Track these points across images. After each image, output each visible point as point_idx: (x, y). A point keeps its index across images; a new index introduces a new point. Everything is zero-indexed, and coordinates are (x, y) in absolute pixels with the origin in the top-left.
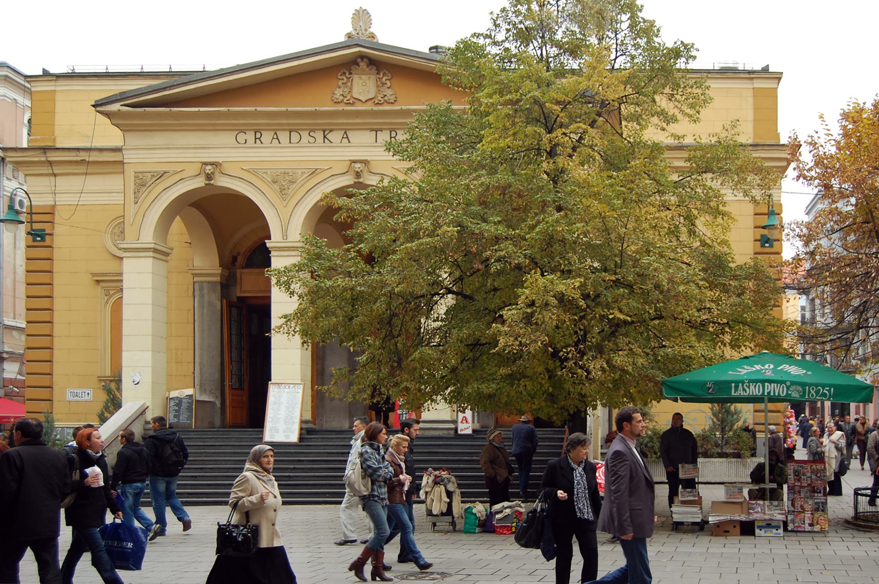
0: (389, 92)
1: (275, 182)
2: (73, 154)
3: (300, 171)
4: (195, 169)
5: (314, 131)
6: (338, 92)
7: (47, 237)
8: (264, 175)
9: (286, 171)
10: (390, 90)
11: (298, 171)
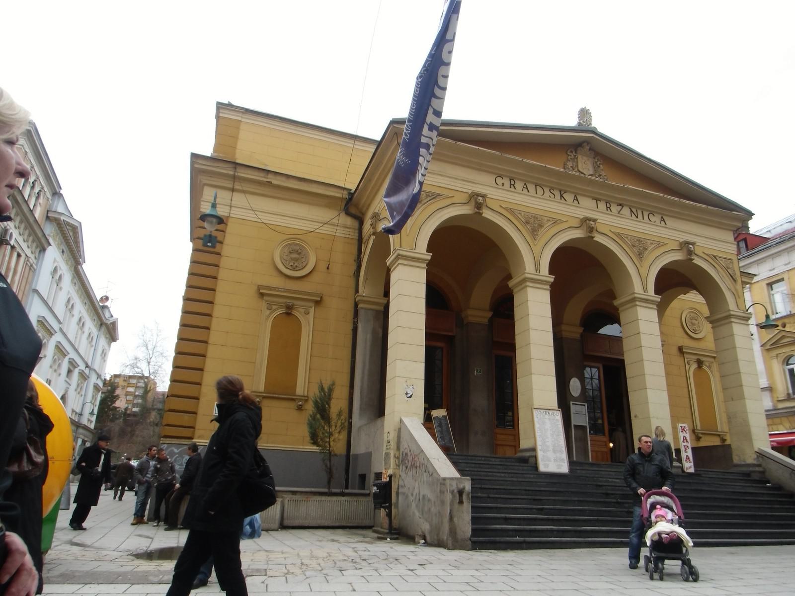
0: (603, 173)
1: (527, 223)
2: (262, 174)
4: (463, 198)
6: (570, 164)
7: (218, 245)
9: (536, 216)
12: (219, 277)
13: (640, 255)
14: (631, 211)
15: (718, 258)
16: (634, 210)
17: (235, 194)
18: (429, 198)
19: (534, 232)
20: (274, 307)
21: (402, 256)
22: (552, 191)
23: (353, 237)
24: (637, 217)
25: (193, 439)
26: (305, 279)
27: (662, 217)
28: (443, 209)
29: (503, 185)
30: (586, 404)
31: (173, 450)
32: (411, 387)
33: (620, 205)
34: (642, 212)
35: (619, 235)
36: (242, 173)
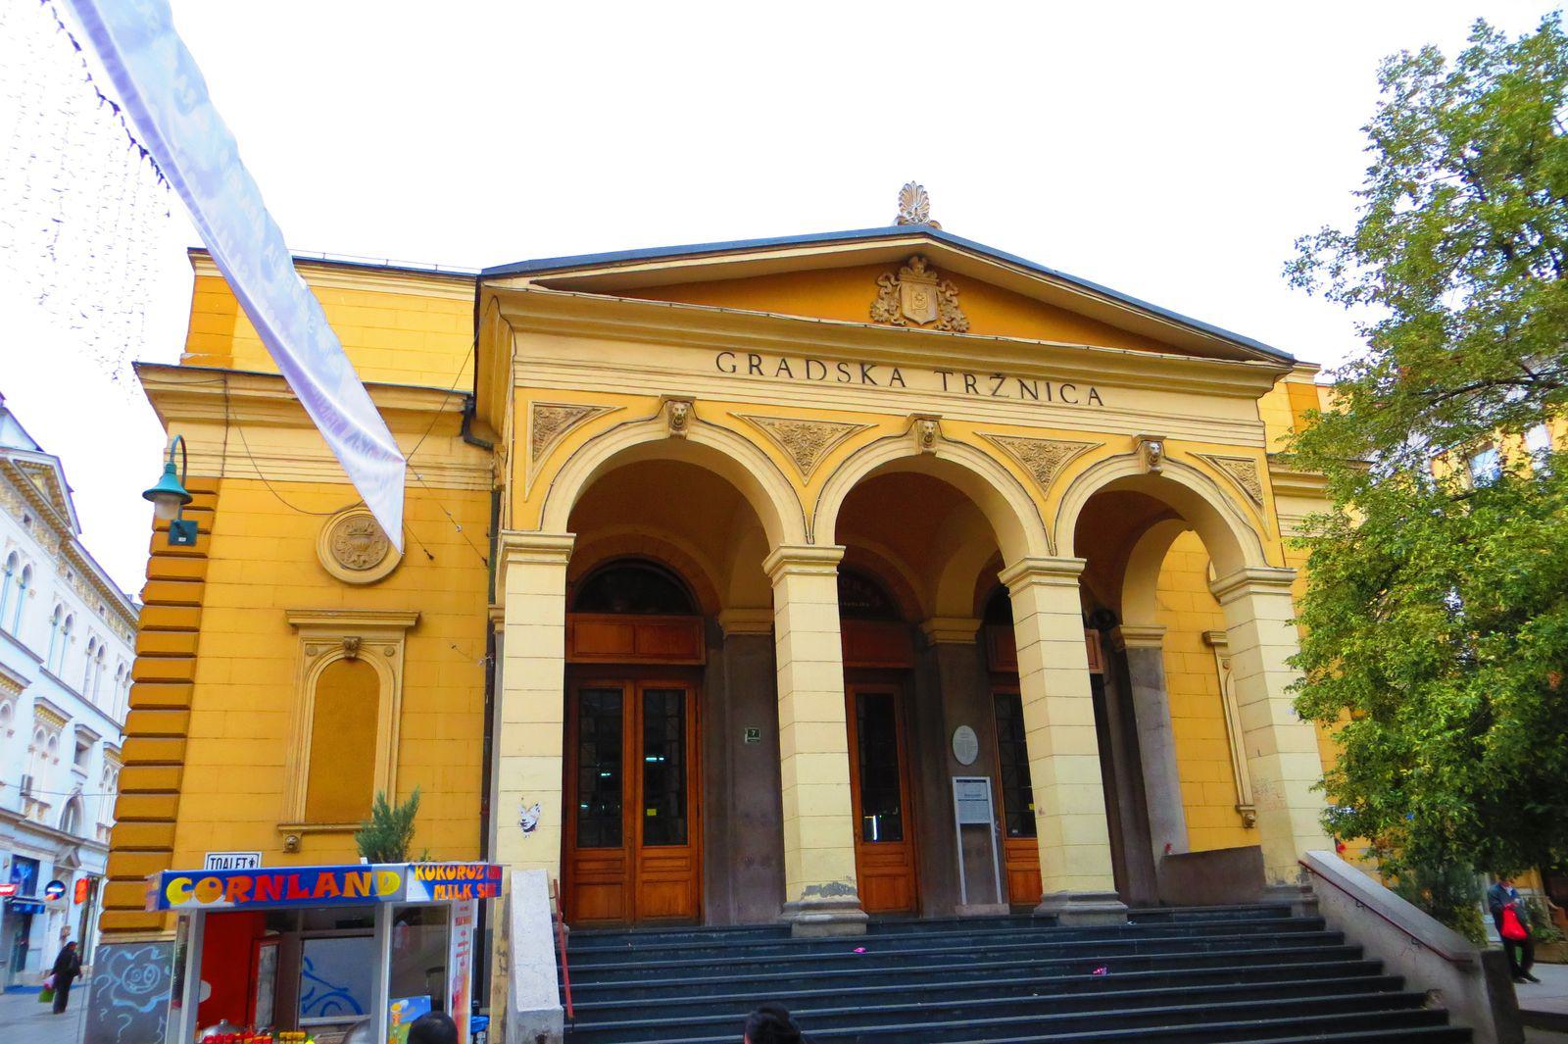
3: (828, 427)
5: (845, 362)
6: (882, 306)
7: (200, 538)
8: (769, 428)
9: (807, 424)
10: (959, 311)
11: (825, 426)
12: (205, 604)
13: (1043, 478)
14: (1023, 385)
15: (1220, 462)
16: (1030, 384)
17: (233, 432)
18: (573, 419)
19: (802, 461)
20: (321, 649)
21: (513, 545)
22: (843, 367)
23: (483, 487)
24: (1036, 398)
25: (162, 930)
26: (380, 586)
27: (1093, 390)
28: (602, 438)
29: (734, 371)
30: (988, 779)
31: (123, 955)
32: (533, 810)
33: (998, 376)
34: (1048, 384)
35: (994, 441)
36: (239, 389)
